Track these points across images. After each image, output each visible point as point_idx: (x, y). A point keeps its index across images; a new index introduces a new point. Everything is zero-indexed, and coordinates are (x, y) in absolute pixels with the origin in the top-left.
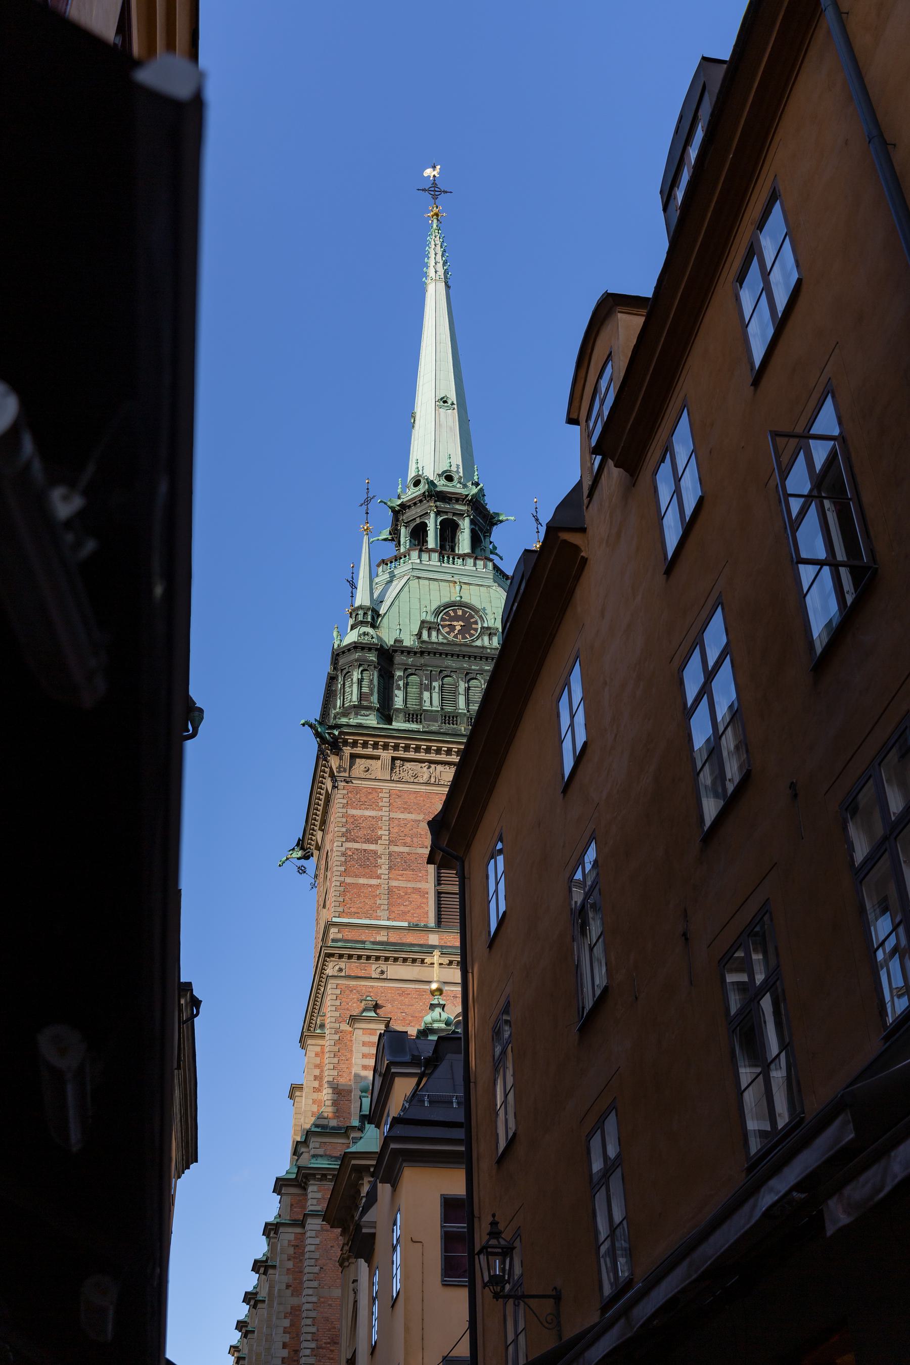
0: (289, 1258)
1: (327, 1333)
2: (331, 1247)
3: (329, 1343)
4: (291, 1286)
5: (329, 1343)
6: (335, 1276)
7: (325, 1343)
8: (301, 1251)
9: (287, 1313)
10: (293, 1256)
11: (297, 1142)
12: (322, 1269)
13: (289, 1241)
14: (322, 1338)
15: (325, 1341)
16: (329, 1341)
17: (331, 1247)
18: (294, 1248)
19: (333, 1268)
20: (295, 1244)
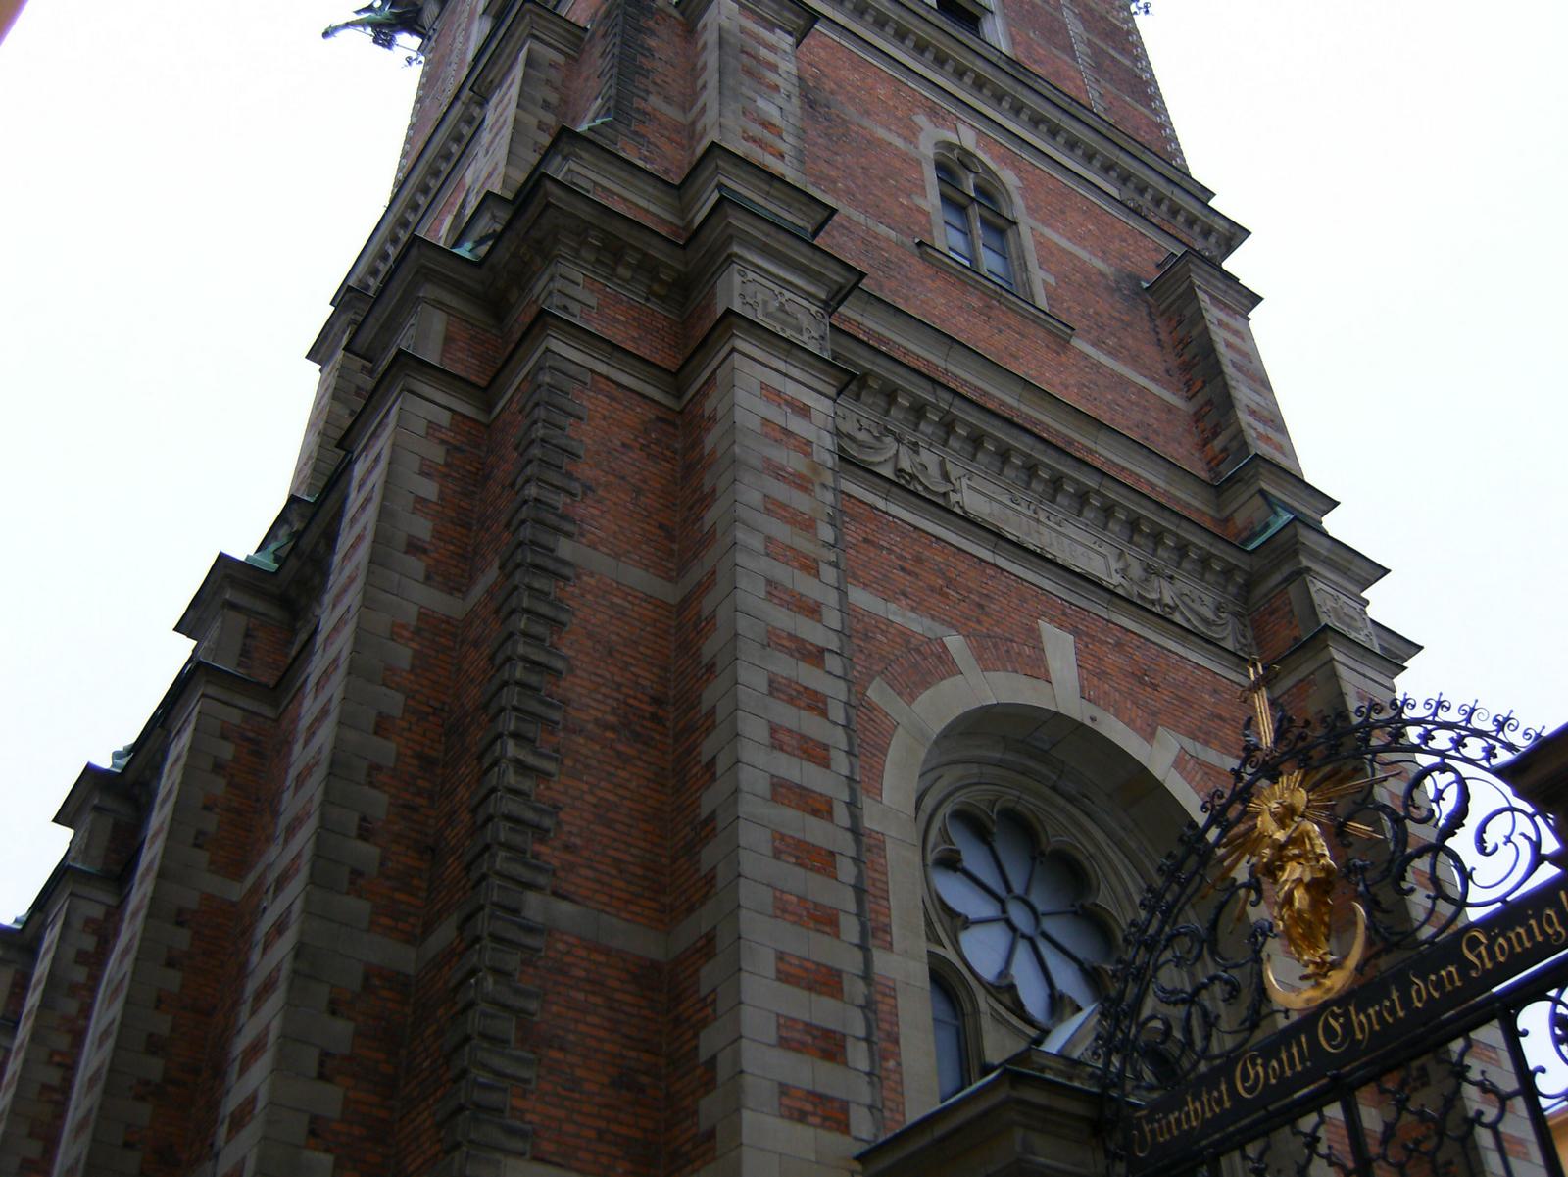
0: (426, 469)
1: (603, 690)
2: (624, 445)
3: (613, 728)
4: (425, 551)
5: (613, 728)
6: (636, 529)
7: (596, 721)
8: (474, 470)
9: (403, 627)
10: (445, 470)
11: (489, 194)
12: (590, 494)
13: (432, 426)
14: (585, 700)
15: (599, 715)
16: (612, 719)
17: (624, 445)
18: (448, 451)
19: (631, 507)
20: (451, 441)
